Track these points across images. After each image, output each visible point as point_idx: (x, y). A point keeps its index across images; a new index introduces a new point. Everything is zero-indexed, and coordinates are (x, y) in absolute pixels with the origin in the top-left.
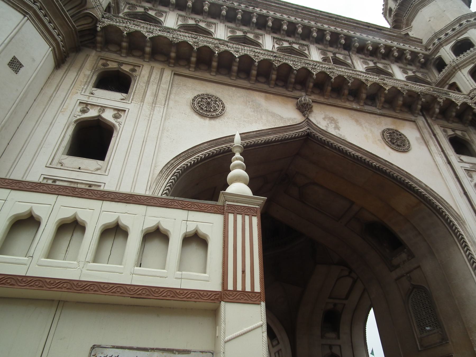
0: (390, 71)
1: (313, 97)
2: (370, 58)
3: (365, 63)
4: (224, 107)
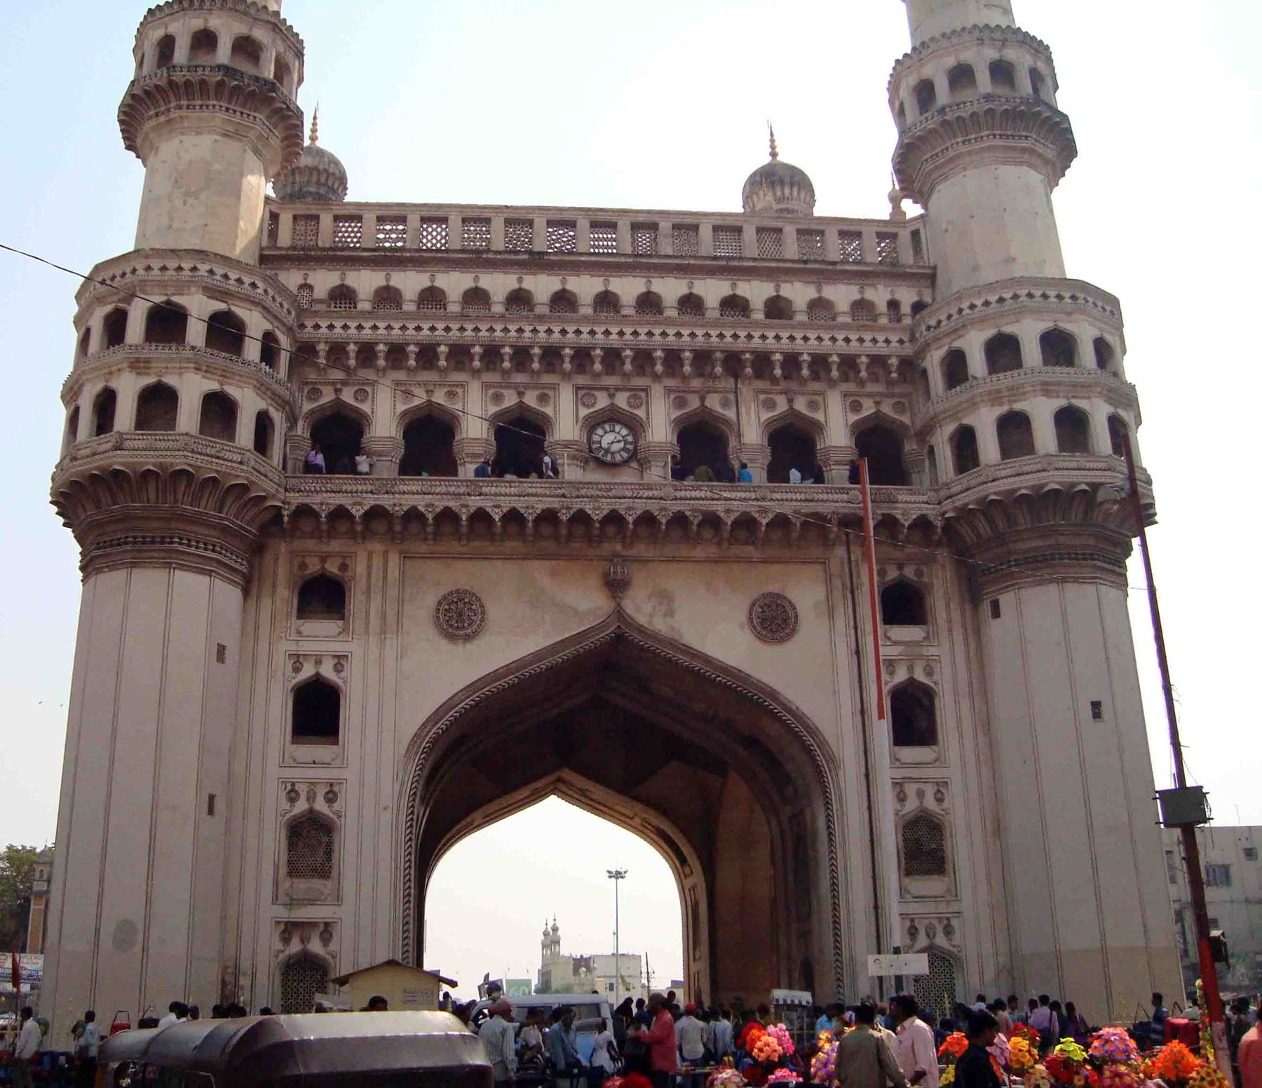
0: (819, 416)
2: (783, 385)
3: (770, 405)
4: (483, 613)
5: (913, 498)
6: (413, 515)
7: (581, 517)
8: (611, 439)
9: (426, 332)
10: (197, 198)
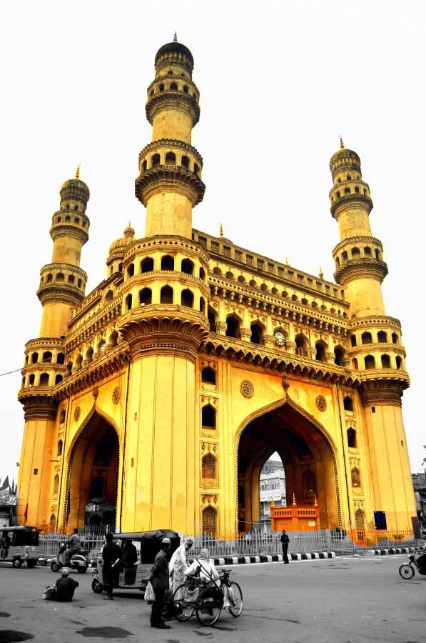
0: (327, 342)
1: (290, 376)
3: (316, 336)
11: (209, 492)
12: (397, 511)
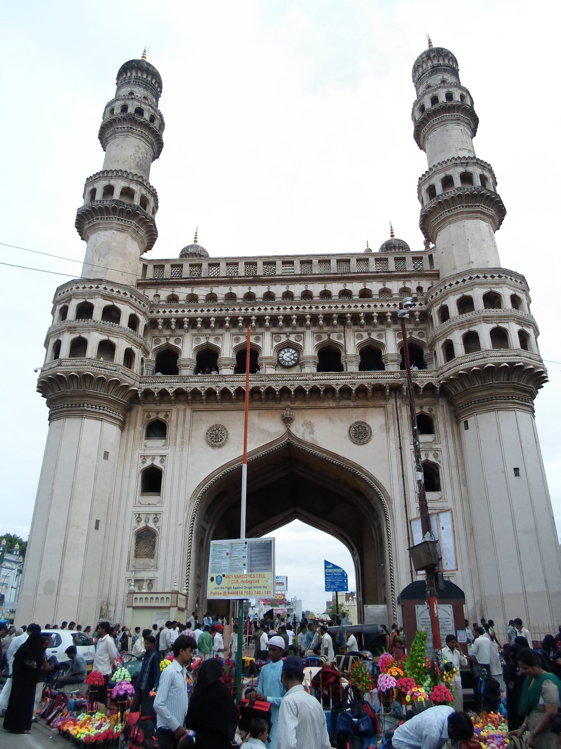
0: (383, 341)
1: (296, 405)
2: (366, 328)
3: (361, 336)
5: (425, 375)
6: (195, 392)
7: (270, 390)
8: (287, 356)
9: (205, 312)
10: (104, 258)
11: (140, 575)
12: (528, 589)
